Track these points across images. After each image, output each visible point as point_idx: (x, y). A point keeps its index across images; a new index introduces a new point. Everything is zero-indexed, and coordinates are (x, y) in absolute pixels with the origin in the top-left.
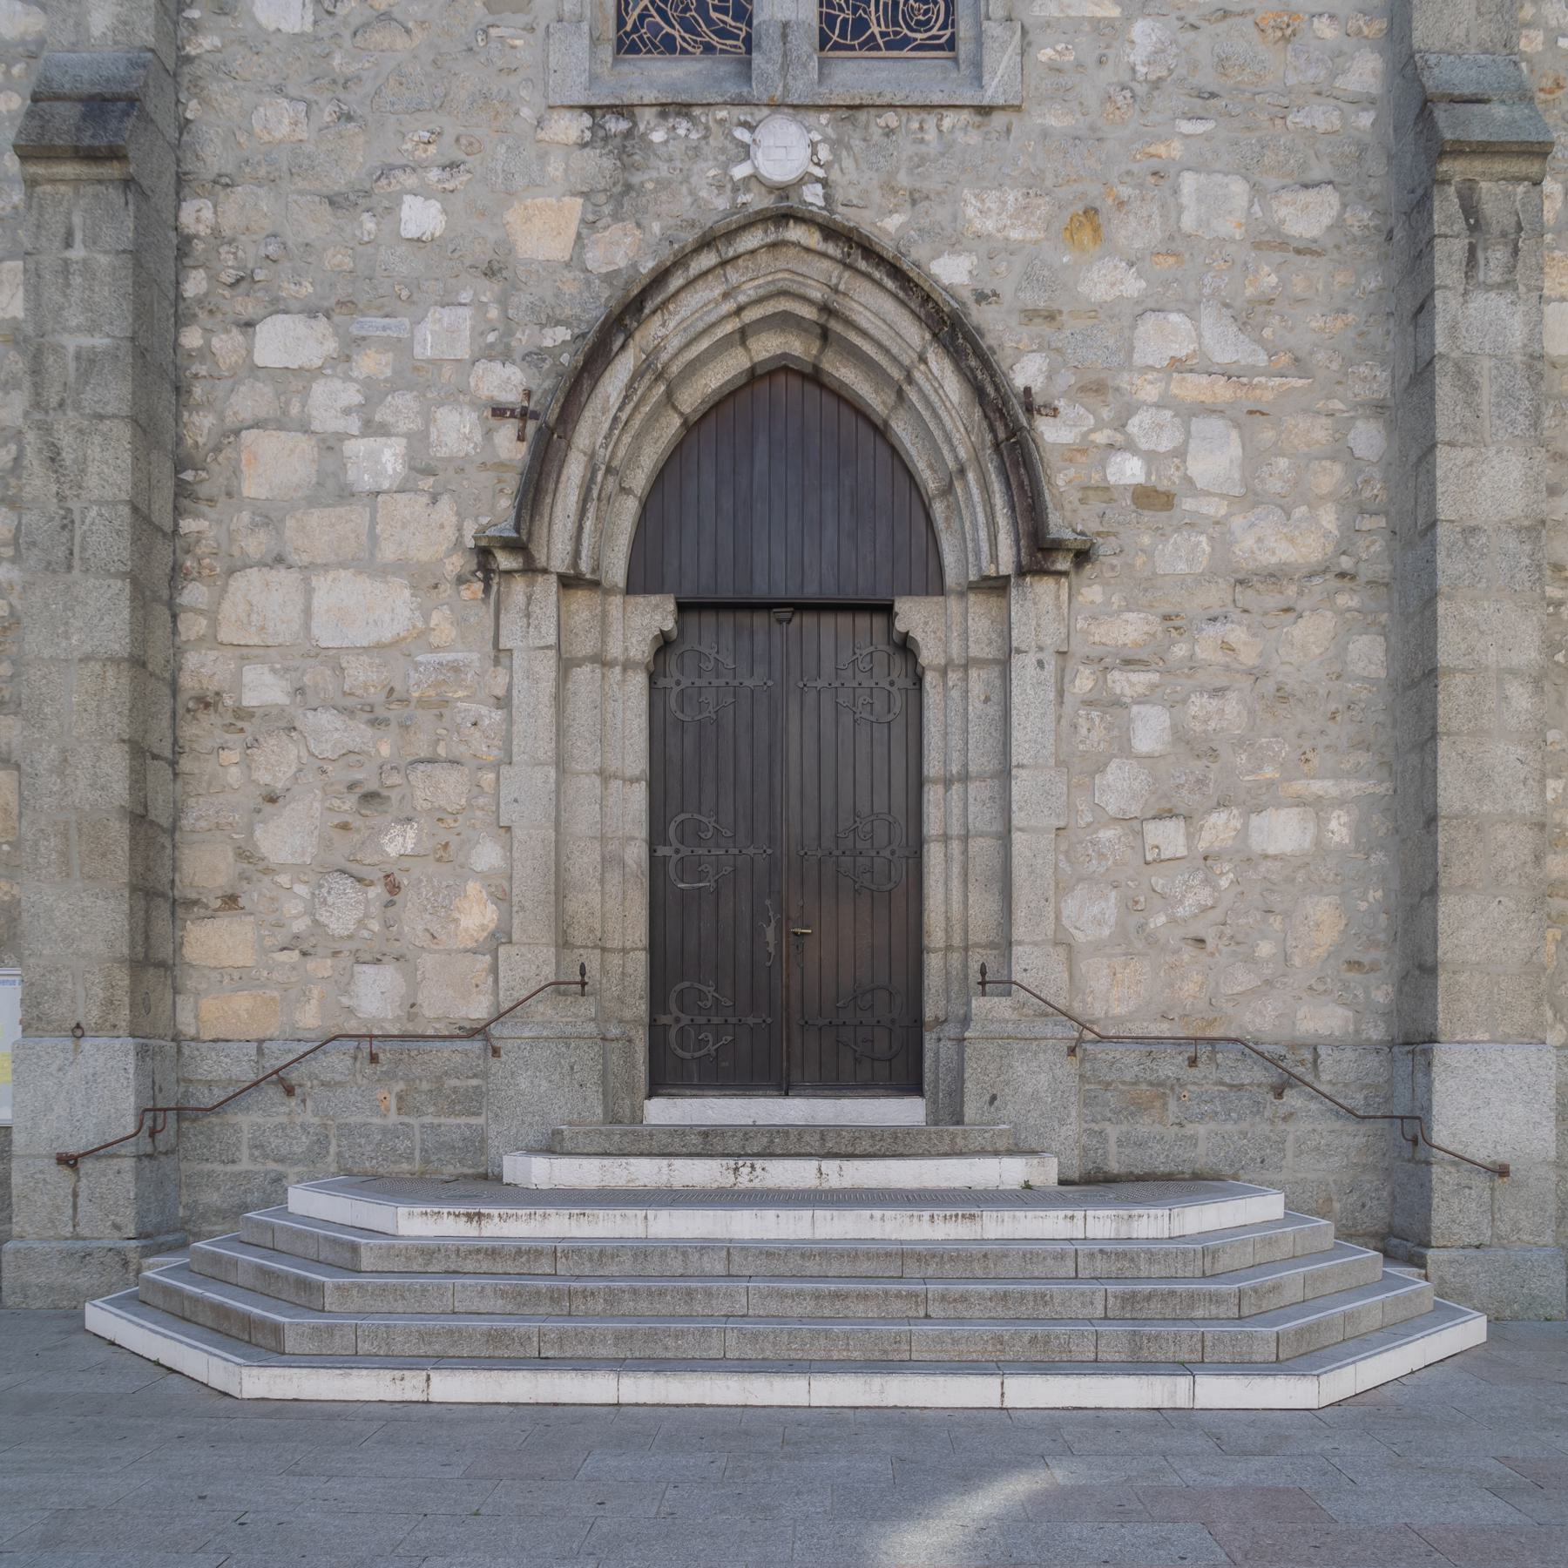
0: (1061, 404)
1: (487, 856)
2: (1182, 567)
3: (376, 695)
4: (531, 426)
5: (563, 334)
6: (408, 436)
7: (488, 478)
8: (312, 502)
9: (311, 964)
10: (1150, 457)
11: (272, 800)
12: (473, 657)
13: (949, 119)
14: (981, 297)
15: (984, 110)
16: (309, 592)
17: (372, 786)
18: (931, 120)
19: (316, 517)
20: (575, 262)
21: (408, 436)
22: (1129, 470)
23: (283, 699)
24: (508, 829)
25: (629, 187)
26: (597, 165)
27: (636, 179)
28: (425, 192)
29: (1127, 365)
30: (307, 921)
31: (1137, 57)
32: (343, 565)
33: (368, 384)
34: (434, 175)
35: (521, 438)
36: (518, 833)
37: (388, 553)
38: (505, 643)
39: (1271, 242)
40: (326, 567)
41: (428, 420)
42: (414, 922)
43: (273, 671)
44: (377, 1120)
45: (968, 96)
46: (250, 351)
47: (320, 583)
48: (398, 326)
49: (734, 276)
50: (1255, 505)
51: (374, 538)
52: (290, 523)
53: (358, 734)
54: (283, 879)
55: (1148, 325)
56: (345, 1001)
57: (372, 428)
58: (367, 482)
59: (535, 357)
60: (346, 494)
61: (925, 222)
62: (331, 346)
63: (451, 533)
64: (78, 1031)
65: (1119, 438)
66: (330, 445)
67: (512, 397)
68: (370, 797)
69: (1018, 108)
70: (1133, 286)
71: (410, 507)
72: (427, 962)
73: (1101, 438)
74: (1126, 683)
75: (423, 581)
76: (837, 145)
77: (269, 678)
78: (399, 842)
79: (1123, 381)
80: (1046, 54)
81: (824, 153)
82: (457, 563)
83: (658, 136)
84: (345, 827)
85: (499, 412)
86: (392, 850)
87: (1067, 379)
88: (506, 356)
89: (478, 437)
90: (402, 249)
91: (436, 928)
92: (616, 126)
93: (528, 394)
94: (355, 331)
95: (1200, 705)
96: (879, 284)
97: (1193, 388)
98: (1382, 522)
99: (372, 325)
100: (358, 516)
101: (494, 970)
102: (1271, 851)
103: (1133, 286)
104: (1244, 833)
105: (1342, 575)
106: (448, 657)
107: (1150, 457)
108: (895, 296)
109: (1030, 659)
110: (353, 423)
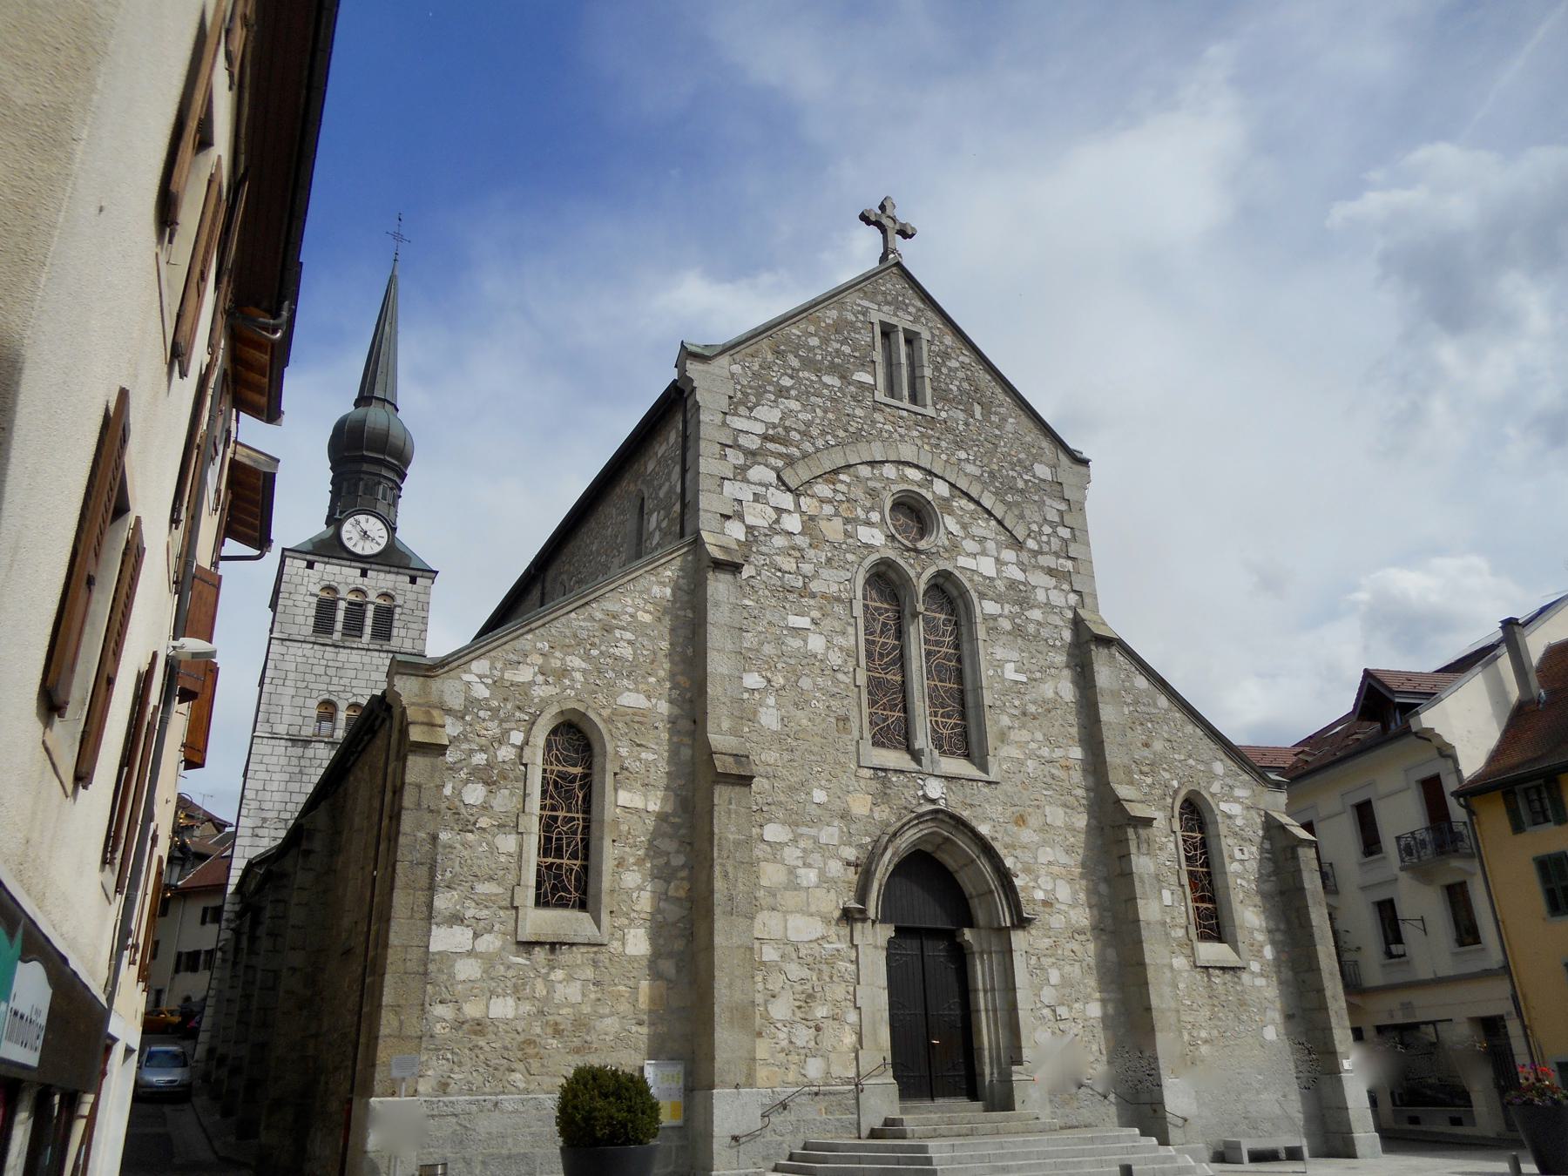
0: (1019, 873)
1: (852, 1017)
2: (1058, 926)
3: (810, 960)
4: (859, 869)
5: (868, 839)
6: (819, 868)
7: (846, 885)
8: (786, 889)
9: (790, 1058)
10: (1045, 890)
11: (774, 997)
12: (843, 945)
13: (980, 784)
14: (993, 839)
15: (989, 783)
16: (786, 921)
17: (811, 991)
18: (975, 783)
19: (788, 894)
20: (871, 816)
21: (819, 868)
22: (1040, 895)
23: (779, 959)
24: (859, 1008)
25: (885, 794)
26: (875, 785)
27: (888, 791)
28: (821, 787)
29: (1036, 862)
30: (787, 1041)
31: (1030, 770)
32: (798, 912)
33: (804, 850)
34: (823, 783)
35: (856, 873)
36: (863, 1009)
37: (813, 909)
38: (855, 943)
39: (1071, 829)
40: (792, 912)
41: (825, 864)
42: (827, 1040)
43: (774, 948)
44: (818, 1118)
45: (984, 776)
46: (762, 835)
47: (790, 918)
48: (813, 832)
49: (921, 826)
50: (1075, 907)
51: (808, 904)
52: (779, 896)
53: (805, 973)
54: (779, 1025)
55: (1041, 851)
56: (803, 1072)
57: (807, 865)
58: (805, 884)
59: (860, 846)
60: (797, 888)
61: (975, 814)
62: (791, 836)
63: (834, 903)
64: (737, 1086)
65: (1036, 885)
66: (792, 871)
67: (853, 859)
68: (810, 996)
69: (997, 783)
70: (1036, 838)
71: (820, 893)
72: (832, 1056)
73: (1032, 884)
74: (1046, 961)
75: (826, 920)
76: (947, 788)
77: (772, 951)
78: (820, 1011)
79: (1035, 867)
80: (1005, 767)
81: (945, 791)
82: (837, 914)
83: (894, 779)
84: (799, 1007)
85: (849, 864)
86: (819, 1015)
87: (1019, 866)
88: (850, 845)
89: (842, 871)
90: (814, 806)
91: (835, 1044)
92: (881, 774)
93: (858, 858)
94: (799, 831)
95: (1067, 969)
96: (964, 833)
97: (1055, 869)
98: (1110, 914)
99: (803, 830)
100: (803, 895)
101: (857, 1058)
102: (1093, 1016)
103: (1036, 838)
104: (1084, 1011)
105: (1102, 930)
106: (835, 946)
107: (1045, 890)
108: (970, 838)
109: (1019, 953)
110: (800, 863)
